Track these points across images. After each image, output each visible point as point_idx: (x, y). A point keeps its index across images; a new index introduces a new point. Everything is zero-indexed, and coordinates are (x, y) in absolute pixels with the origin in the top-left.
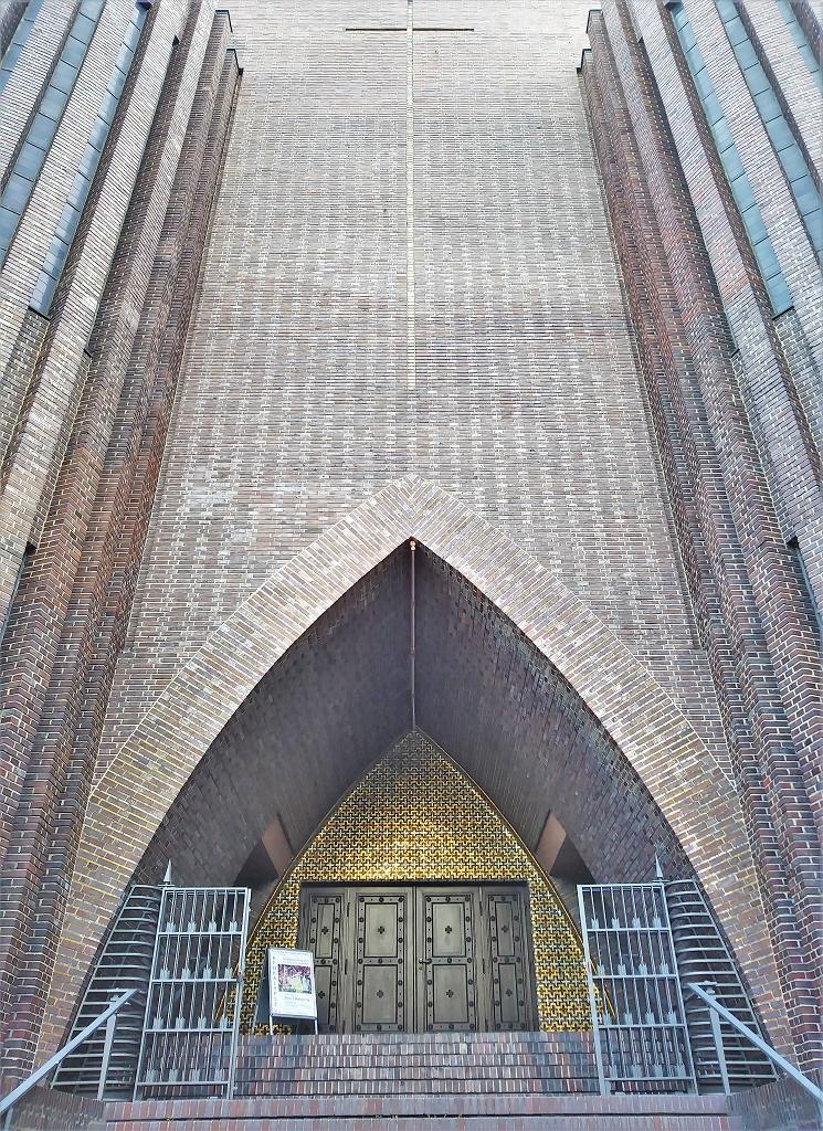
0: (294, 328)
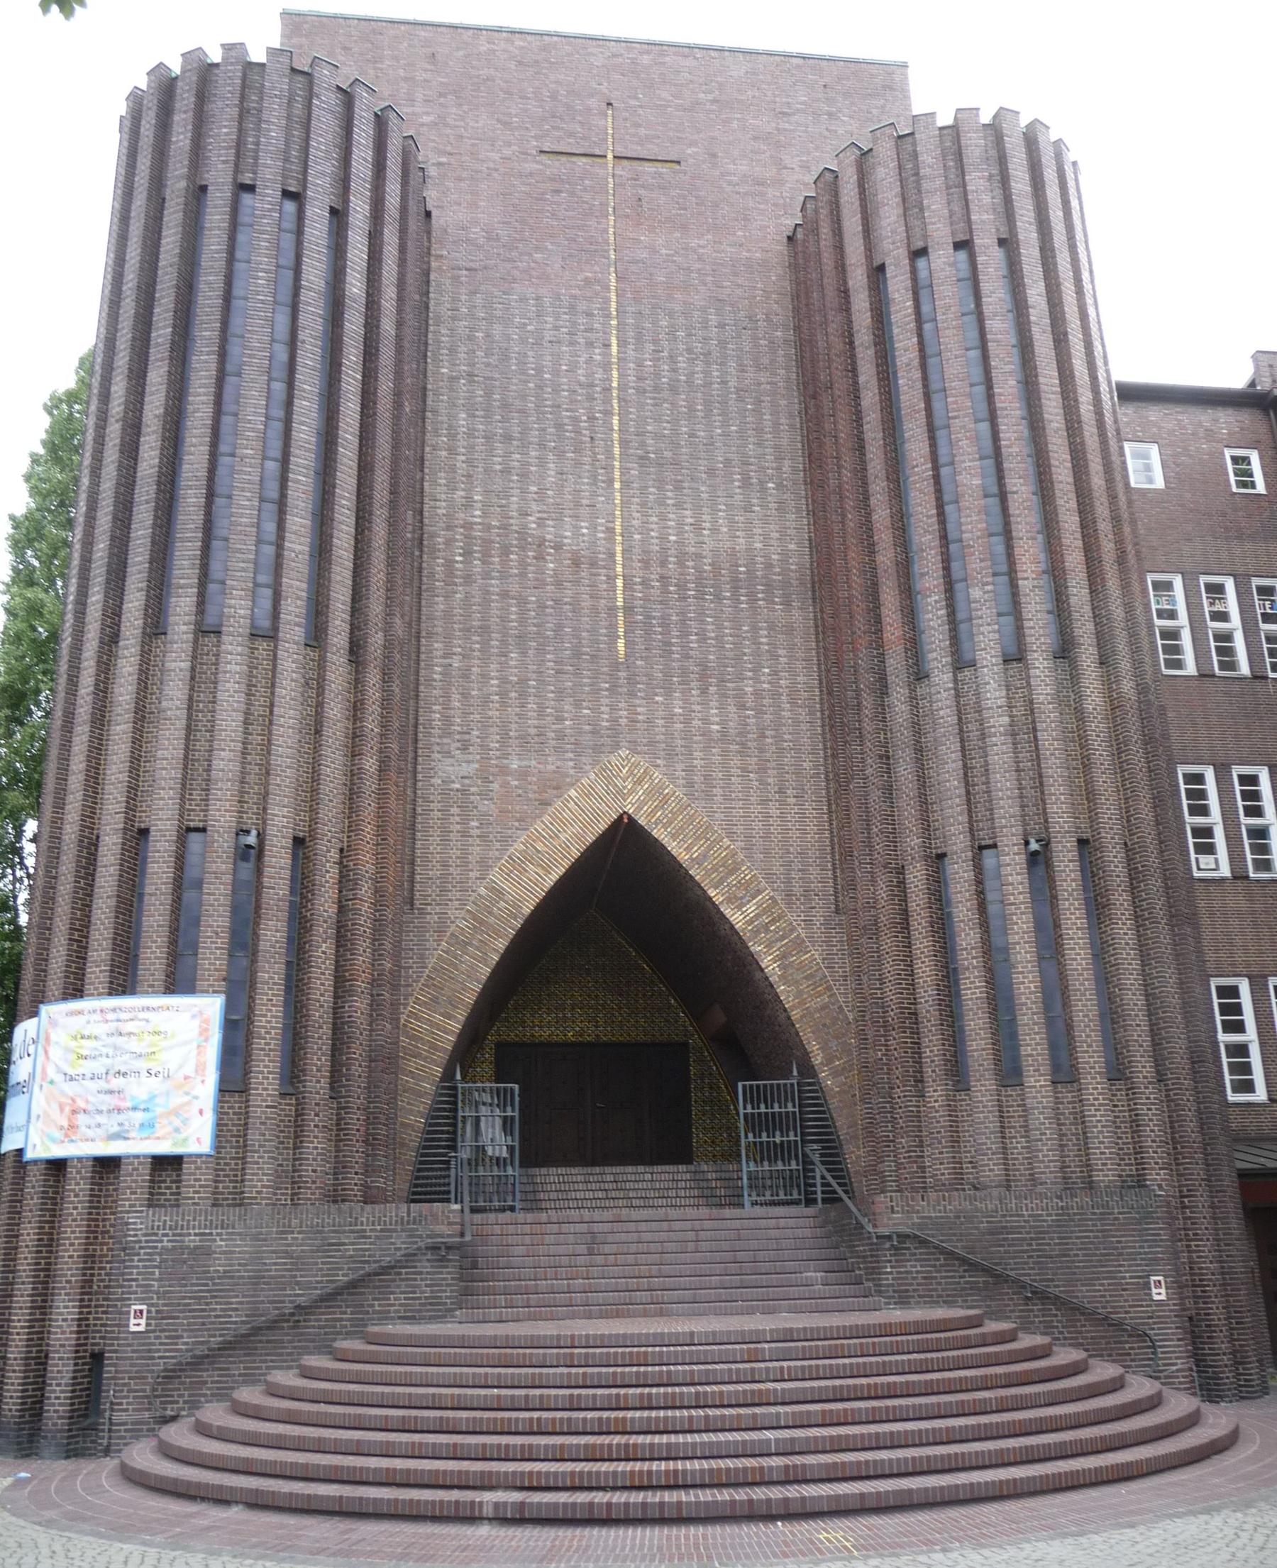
0: (514, 588)
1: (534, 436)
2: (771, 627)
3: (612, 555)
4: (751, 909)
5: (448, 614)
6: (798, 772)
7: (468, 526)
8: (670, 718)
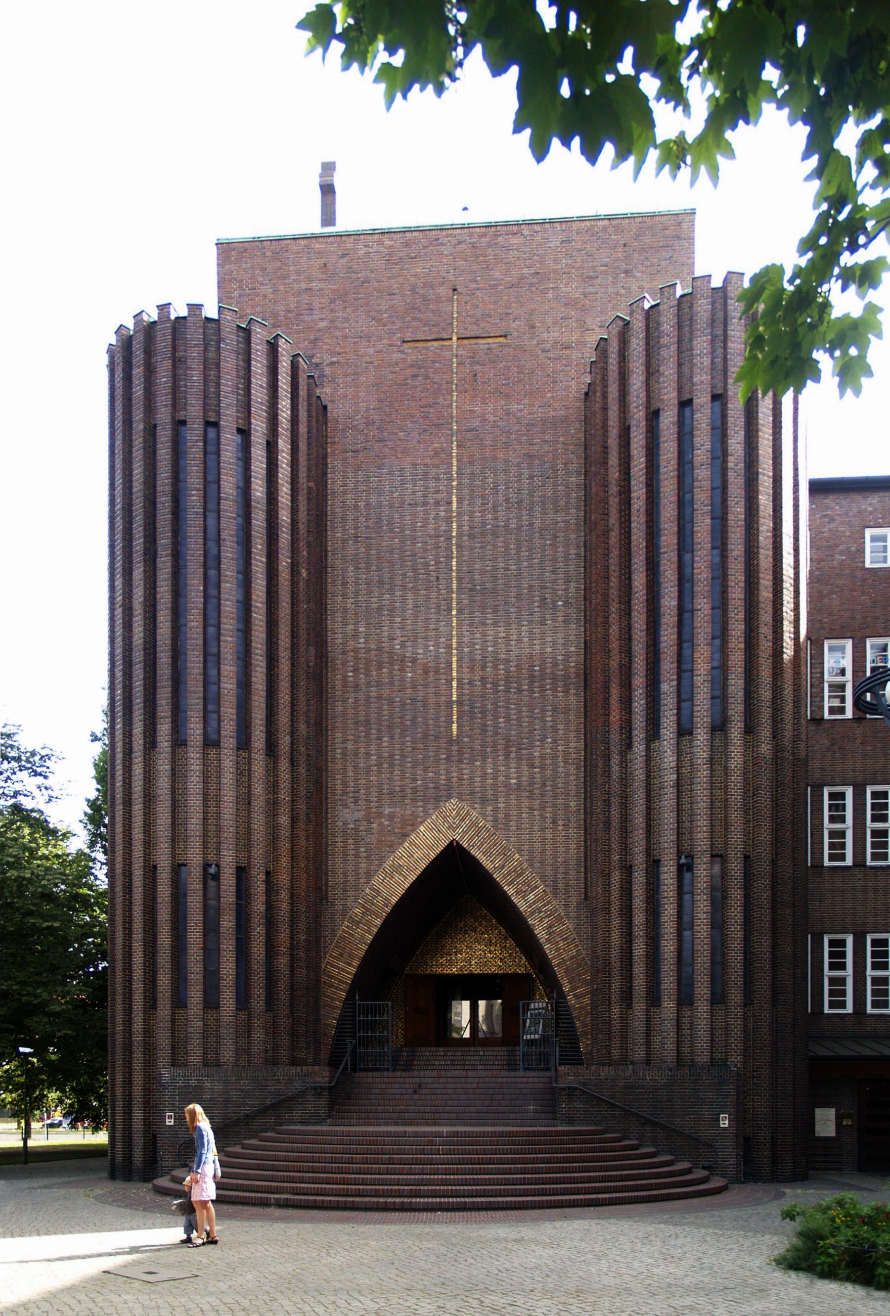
0: (386, 693)
1: (398, 581)
2: (554, 710)
3: (450, 664)
4: (531, 896)
5: (344, 713)
6: (567, 806)
7: (356, 650)
8: (484, 776)
